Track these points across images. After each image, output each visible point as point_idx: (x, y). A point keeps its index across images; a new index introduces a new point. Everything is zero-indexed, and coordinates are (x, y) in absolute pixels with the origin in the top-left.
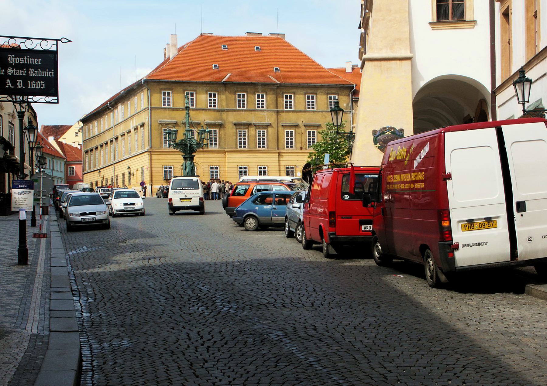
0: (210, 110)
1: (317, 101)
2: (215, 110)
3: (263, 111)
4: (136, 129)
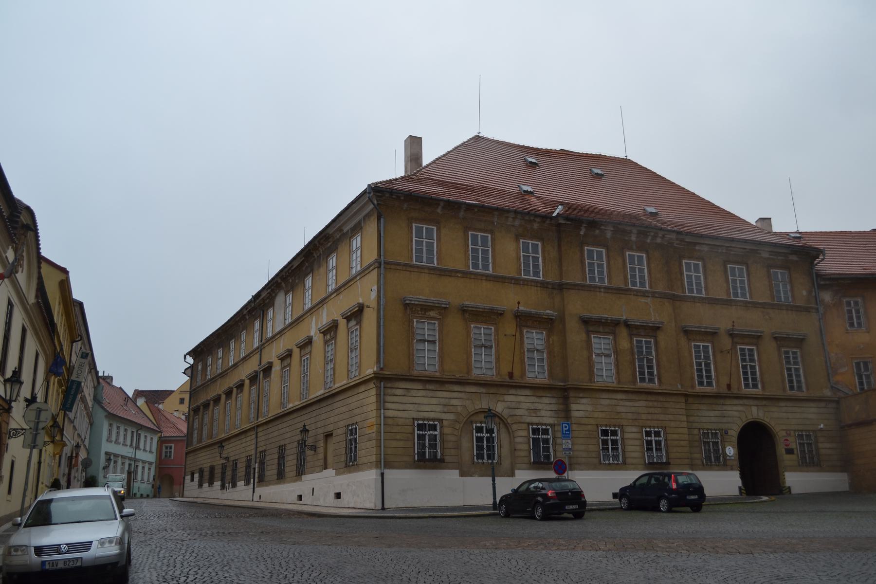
0: (527, 283)
1: (749, 280)
3: (644, 294)
4: (331, 330)
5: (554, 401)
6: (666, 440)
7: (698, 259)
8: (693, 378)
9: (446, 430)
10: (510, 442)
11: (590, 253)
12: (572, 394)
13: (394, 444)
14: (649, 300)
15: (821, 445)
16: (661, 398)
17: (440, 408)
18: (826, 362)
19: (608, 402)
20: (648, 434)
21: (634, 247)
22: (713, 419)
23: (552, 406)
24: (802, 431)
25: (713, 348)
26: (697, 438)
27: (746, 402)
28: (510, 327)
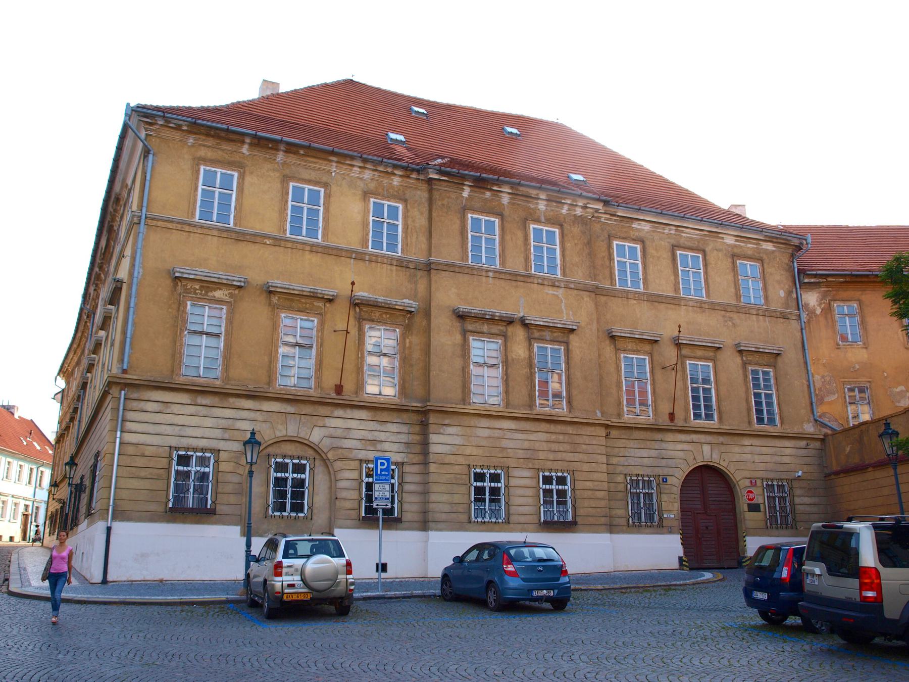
0: (374, 259)
1: (706, 273)
2: (390, 261)
3: (554, 285)
5: (404, 429)
6: (573, 490)
7: (634, 240)
8: (620, 404)
9: (223, 467)
10: (330, 488)
11: (477, 222)
12: (432, 419)
13: (135, 483)
14: (560, 292)
15: (797, 500)
16: (570, 429)
17: (218, 433)
18: (809, 386)
19: (487, 433)
20: (548, 480)
21: (543, 219)
22: (646, 462)
23: (403, 436)
24: (772, 480)
25: (652, 362)
26: (621, 487)
27: (694, 437)
28: (340, 318)
